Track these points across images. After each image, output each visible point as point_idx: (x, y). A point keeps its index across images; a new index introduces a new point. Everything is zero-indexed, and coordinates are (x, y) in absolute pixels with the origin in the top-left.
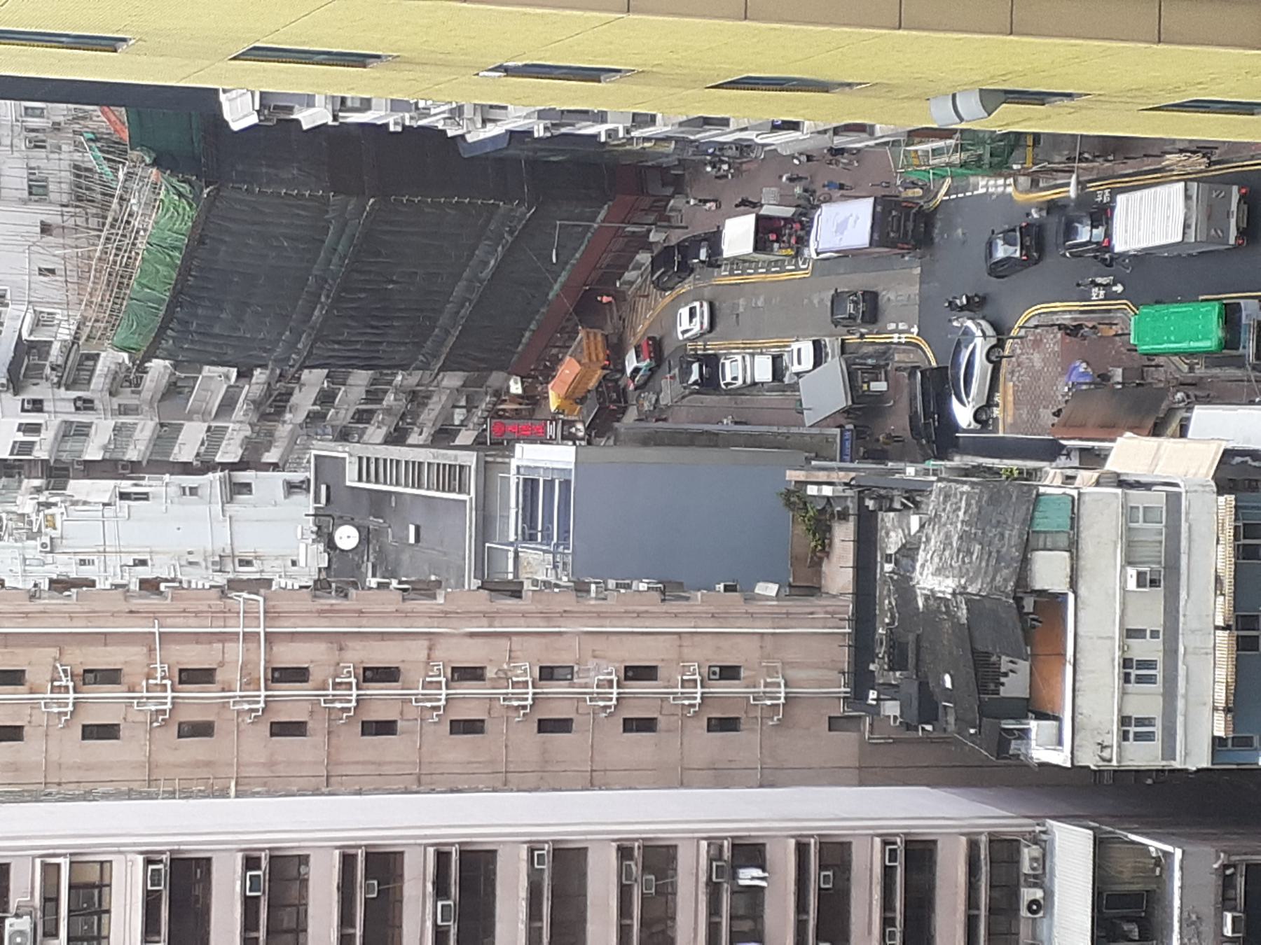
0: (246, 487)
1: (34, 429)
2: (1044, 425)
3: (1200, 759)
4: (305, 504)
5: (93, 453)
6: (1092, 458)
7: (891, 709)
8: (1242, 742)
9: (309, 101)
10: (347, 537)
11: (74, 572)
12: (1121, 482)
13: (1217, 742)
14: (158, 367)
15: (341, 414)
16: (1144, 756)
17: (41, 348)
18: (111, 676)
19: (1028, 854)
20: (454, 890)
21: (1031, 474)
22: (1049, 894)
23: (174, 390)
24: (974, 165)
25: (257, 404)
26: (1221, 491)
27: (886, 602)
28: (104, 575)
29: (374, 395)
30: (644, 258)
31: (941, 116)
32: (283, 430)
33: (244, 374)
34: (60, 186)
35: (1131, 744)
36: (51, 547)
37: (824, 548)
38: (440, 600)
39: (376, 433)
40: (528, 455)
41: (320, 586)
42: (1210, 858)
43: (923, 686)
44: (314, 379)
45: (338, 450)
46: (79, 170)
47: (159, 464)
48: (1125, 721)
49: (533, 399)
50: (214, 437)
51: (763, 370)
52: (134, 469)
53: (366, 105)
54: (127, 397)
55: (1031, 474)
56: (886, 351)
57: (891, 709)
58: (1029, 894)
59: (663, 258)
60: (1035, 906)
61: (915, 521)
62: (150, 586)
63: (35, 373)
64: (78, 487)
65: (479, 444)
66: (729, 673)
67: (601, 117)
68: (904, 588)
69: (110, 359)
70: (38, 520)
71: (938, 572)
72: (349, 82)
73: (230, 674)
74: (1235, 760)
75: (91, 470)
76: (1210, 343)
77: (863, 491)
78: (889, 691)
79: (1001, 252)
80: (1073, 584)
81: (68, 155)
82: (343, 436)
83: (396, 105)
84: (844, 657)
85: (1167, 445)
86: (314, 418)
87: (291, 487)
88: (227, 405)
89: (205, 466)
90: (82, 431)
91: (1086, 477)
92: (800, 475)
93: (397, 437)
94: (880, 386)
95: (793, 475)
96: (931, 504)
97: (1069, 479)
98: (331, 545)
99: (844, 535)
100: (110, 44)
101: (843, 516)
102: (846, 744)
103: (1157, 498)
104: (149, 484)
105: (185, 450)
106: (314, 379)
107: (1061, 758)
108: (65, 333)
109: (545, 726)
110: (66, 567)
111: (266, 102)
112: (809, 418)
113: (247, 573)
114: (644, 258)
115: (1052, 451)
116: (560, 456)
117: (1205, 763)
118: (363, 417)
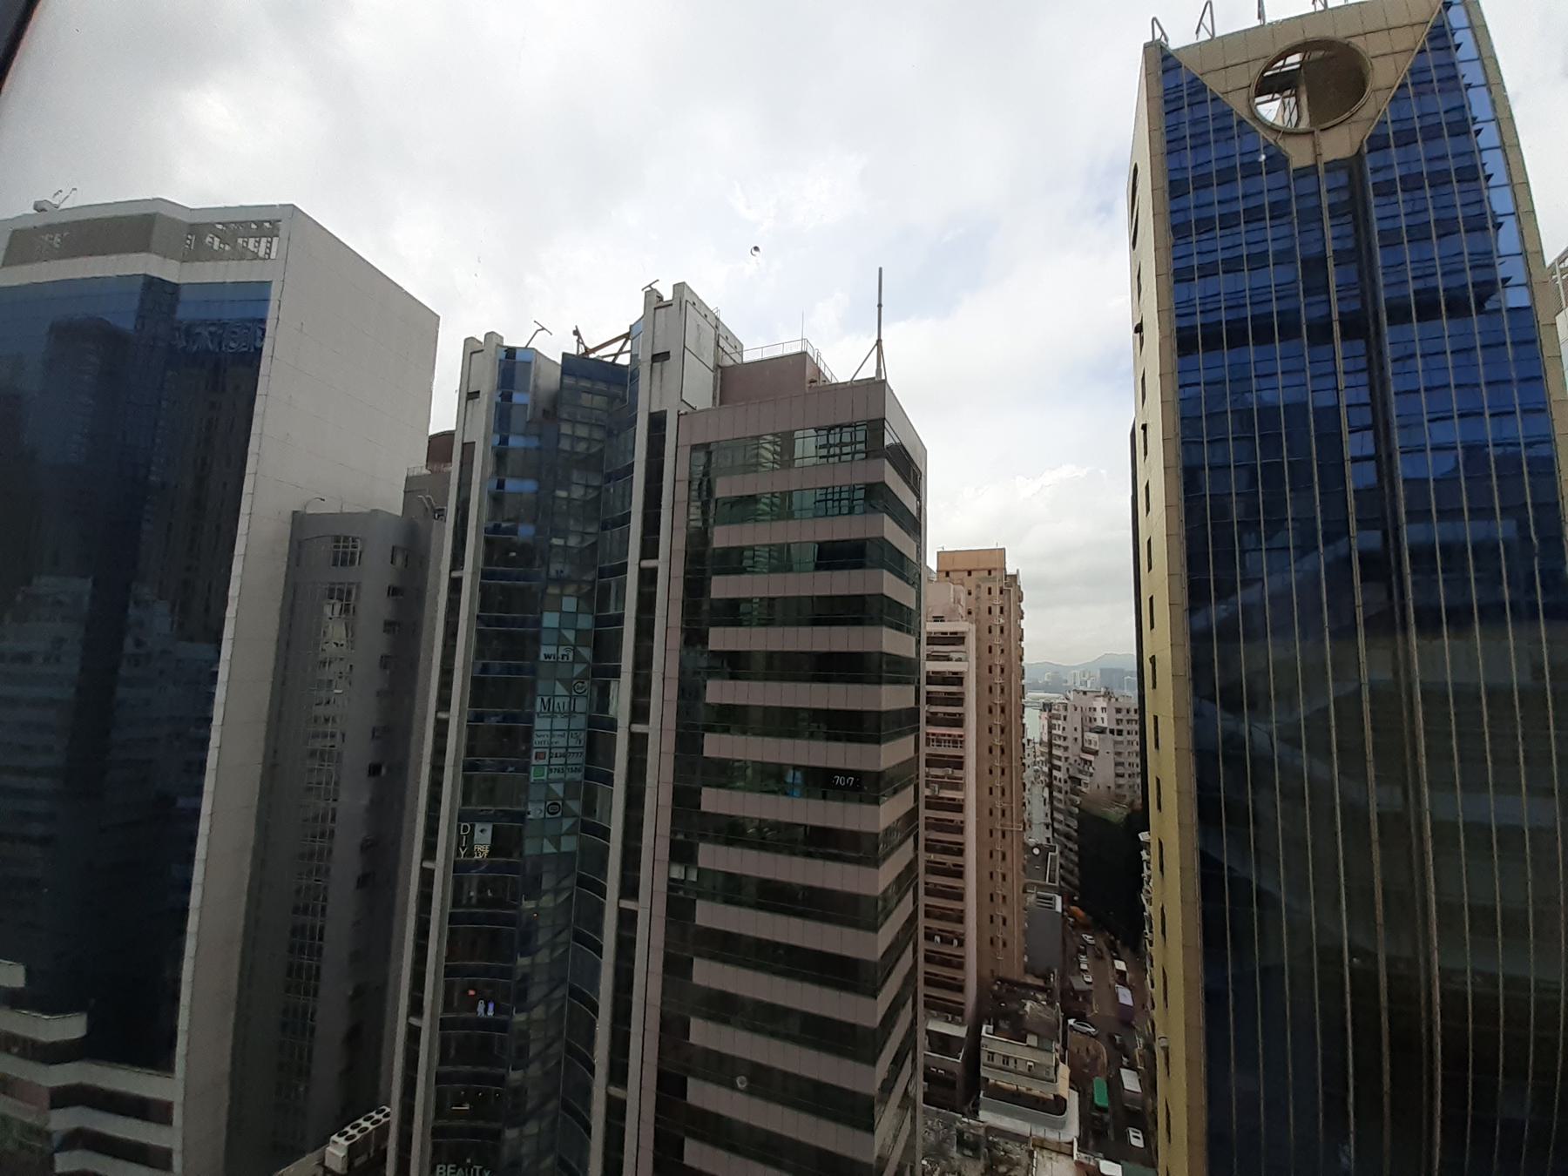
1: (1060, 781)
2: (1072, 1047)
3: (983, 1074)
4: (1045, 843)
5: (1055, 794)
7: (996, 988)
9: (1148, 854)
10: (1036, 851)
11: (1027, 787)
12: (1057, 1066)
13: (988, 1080)
14: (1077, 810)
16: (984, 1058)
18: (1003, 794)
19: (959, 1018)
21: (1058, 1042)
22: (950, 1022)
23: (1071, 814)
29: (1072, 861)
31: (1159, 1033)
32: (1062, 839)
33: (1076, 831)
35: (987, 1054)
36: (1032, 783)
37: (1037, 977)
40: (1059, 899)
41: (1024, 844)
42: (958, 1071)
45: (1057, 852)
47: (1053, 809)
49: (1074, 903)
50: (1060, 822)
51: (1084, 967)
52: (1051, 803)
53: (1149, 868)
54: (1069, 803)
57: (996, 988)
60: (947, 1018)
61: (1044, 1003)
62: (1024, 804)
63: (1073, 782)
64: (1047, 790)
69: (1078, 800)
72: (1155, 864)
74: (983, 1085)
75: (1051, 793)
76: (1096, 1101)
79: (1117, 1037)
80: (1028, 1046)
81: (1127, 794)
82: (1061, 853)
85: (1067, 1083)
86: (1066, 846)
87: (1048, 839)
88: (1068, 826)
89: (1053, 819)
90: (1060, 792)
92: (1056, 972)
93: (1061, 866)
94: (1081, 999)
97: (1057, 1050)
99: (1040, 983)
100: (1159, 807)
101: (1045, 983)
103: (1052, 1076)
104: (1048, 806)
105: (1056, 815)
106: (1076, 847)
107: (983, 1033)
108: (1084, 790)
109: (992, 896)
110: (1028, 786)
112: (1071, 978)
113: (1027, 827)
115: (1064, 1047)
116: (1059, 908)
118: (1067, 858)
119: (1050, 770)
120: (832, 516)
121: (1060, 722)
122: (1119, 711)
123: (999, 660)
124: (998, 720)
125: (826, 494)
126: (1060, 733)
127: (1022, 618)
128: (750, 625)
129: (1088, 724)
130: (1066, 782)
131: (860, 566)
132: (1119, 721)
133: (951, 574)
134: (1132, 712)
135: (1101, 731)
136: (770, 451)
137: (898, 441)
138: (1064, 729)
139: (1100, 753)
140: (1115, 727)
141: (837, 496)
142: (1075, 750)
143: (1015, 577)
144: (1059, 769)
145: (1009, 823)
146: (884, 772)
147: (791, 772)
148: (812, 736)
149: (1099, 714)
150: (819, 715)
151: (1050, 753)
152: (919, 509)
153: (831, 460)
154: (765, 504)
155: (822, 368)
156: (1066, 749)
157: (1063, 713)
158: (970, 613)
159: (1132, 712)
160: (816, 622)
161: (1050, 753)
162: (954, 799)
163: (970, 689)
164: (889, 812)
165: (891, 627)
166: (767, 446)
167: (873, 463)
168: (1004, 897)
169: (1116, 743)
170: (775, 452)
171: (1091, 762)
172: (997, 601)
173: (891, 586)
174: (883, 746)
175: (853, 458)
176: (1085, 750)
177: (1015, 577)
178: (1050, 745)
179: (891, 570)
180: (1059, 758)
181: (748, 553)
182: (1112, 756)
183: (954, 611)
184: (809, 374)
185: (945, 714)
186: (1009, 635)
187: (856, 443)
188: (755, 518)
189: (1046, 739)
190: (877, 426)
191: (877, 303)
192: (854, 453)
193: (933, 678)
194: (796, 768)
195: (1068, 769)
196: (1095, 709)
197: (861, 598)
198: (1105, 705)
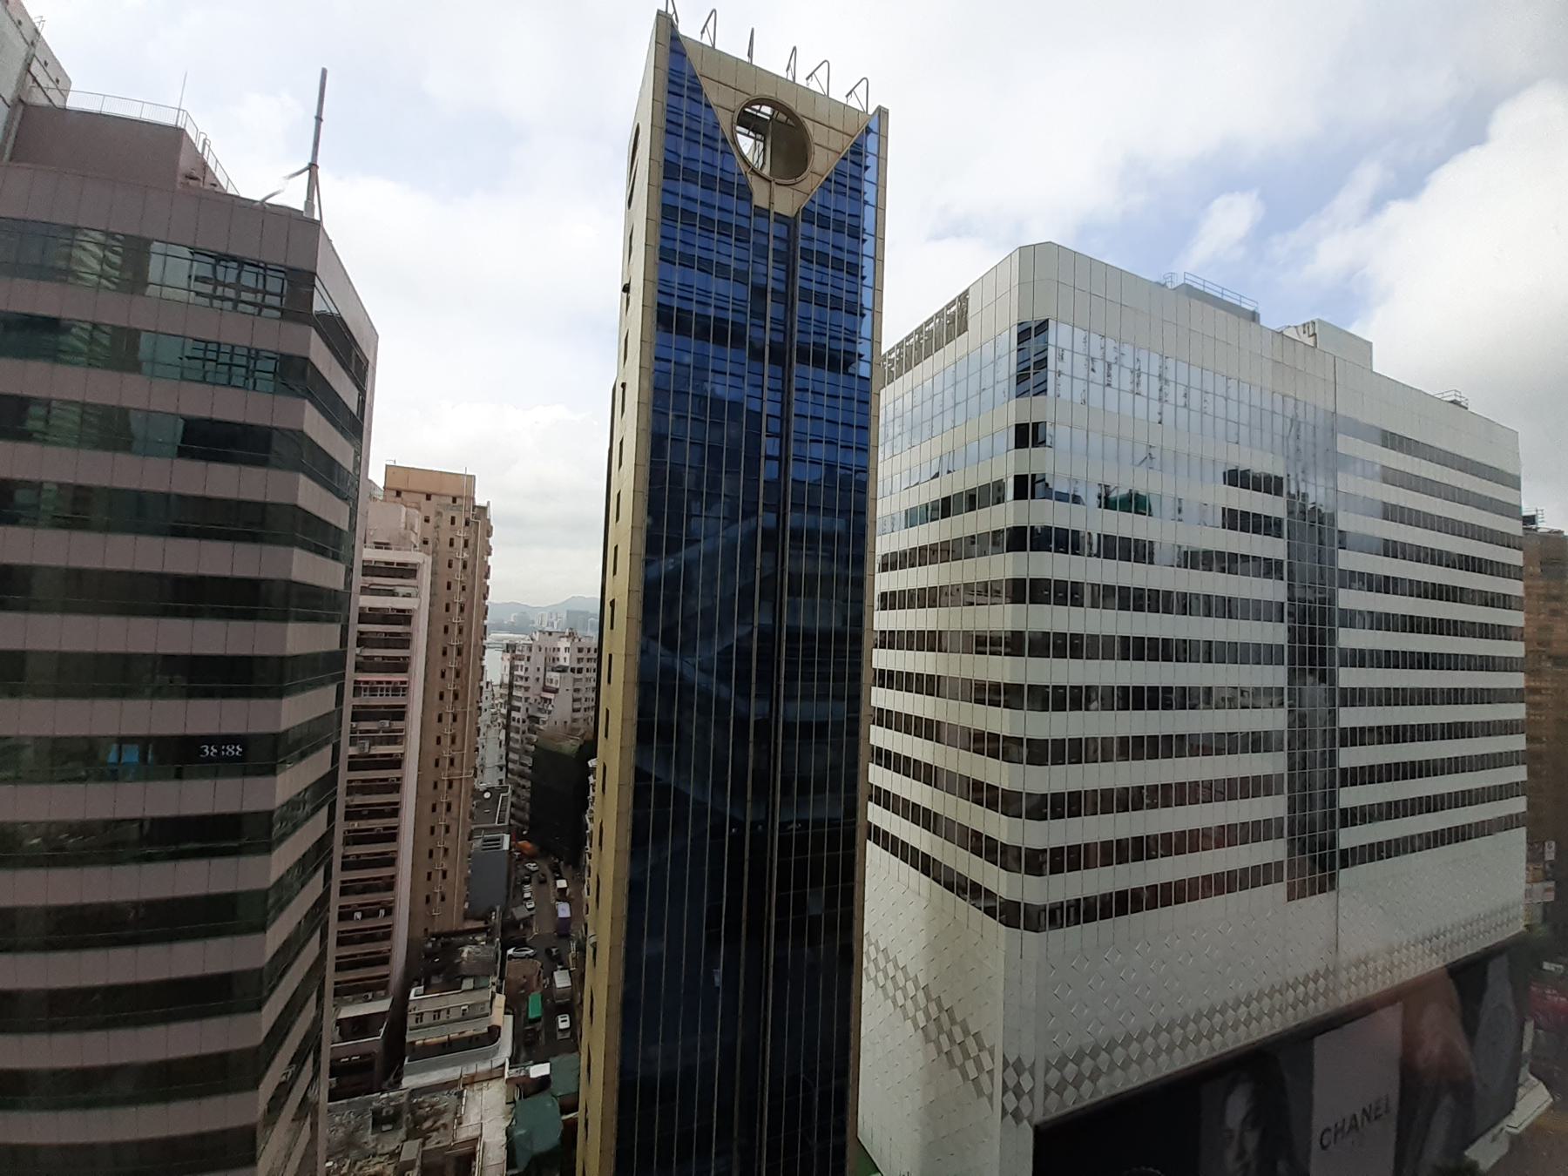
0: (501, 770)
1: (518, 721)
2: (509, 975)
4: (496, 784)
5: (512, 735)
6: (499, 991)
7: (430, 945)
8: (414, 1050)
9: (594, 778)
10: (487, 795)
12: (493, 997)
14: (533, 748)
15: (520, 791)
16: (411, 1022)
17: (538, 723)
19: (382, 993)
20: (387, 832)
22: (370, 1001)
23: (526, 752)
24: (578, 943)
25: (523, 771)
26: (489, 1028)
27: (461, 939)
28: (480, 739)
30: (557, 861)
31: (590, 933)
33: (530, 768)
34: (575, 725)
36: (488, 726)
37: (478, 919)
38: (469, 820)
39: (514, 799)
40: (507, 838)
41: (474, 790)
43: (436, 954)
44: (528, 784)
46: (579, 729)
47: (509, 749)
48: (422, 1014)
49: (523, 838)
50: (514, 762)
51: (527, 895)
53: (594, 791)
54: (525, 741)
55: (496, 974)
56: (531, 927)
57: (430, 945)
58: (370, 995)
59: (557, 865)
62: (477, 750)
64: (503, 732)
65: (510, 825)
66: (443, 899)
67: (591, 846)
68: (464, 945)
69: (535, 738)
70: (496, 723)
71: (469, 953)
73: (452, 769)
74: (408, 1049)
75: (507, 735)
77: (493, 928)
78: (434, 944)
79: (554, 950)
82: (514, 792)
83: (593, 798)
84: (446, 929)
86: (519, 785)
87: (501, 781)
88: (522, 764)
89: (507, 761)
90: (518, 732)
91: (494, 988)
93: (513, 805)
95: (498, 908)
96: (488, 947)
98: (485, 791)
99: (481, 924)
101: (486, 923)
102: (420, 933)
103: (487, 1010)
104: (503, 748)
106: (528, 784)
107: (412, 997)
108: (541, 727)
110: (483, 730)
111: (594, 769)
113: (479, 772)
114: (557, 861)
115: (502, 978)
116: (506, 847)
117: (408, 1039)
118: (519, 796)
119: (509, 713)
120: (214, 384)
121: (523, 663)
122: (580, 650)
123: (459, 599)
124: (453, 663)
125: (206, 350)
126: (522, 673)
127: (489, 554)
128: (33, 523)
129: (552, 664)
130: (524, 722)
131: (263, 463)
132: (580, 660)
133: (403, 495)
134: (592, 651)
135: (563, 670)
136: (94, 256)
137: (334, 311)
138: (526, 669)
139: (560, 691)
140: (576, 666)
141: (224, 358)
142: (536, 689)
143: (484, 509)
144: (518, 709)
145: (459, 772)
146: (287, 731)
147: (115, 747)
148: (158, 693)
149: (562, 654)
150: (171, 663)
151: (510, 694)
152: (362, 403)
153: (217, 303)
154: (80, 339)
155: (211, 164)
156: (527, 689)
157: (526, 654)
158: (425, 542)
159: (592, 651)
160: (178, 532)
161: (510, 694)
162: (390, 755)
163: (420, 631)
164: (290, 782)
165: (302, 547)
166: (89, 246)
167: (295, 329)
168: (446, 850)
169: (576, 680)
170: (104, 261)
171: (550, 700)
172: (461, 533)
173: (309, 495)
174: (283, 701)
175: (260, 311)
176: (545, 689)
177: (484, 509)
178: (511, 686)
179: (312, 476)
180: (519, 699)
181: (35, 410)
182: (571, 692)
183: (405, 538)
184: (185, 163)
185: (383, 658)
186: (473, 573)
187: (265, 293)
188: (54, 355)
189: (506, 680)
190: (302, 280)
191: (315, 113)
192: (261, 307)
193: (365, 617)
194: (122, 741)
195: (527, 710)
196: (559, 649)
197: (263, 507)
198: (568, 645)
